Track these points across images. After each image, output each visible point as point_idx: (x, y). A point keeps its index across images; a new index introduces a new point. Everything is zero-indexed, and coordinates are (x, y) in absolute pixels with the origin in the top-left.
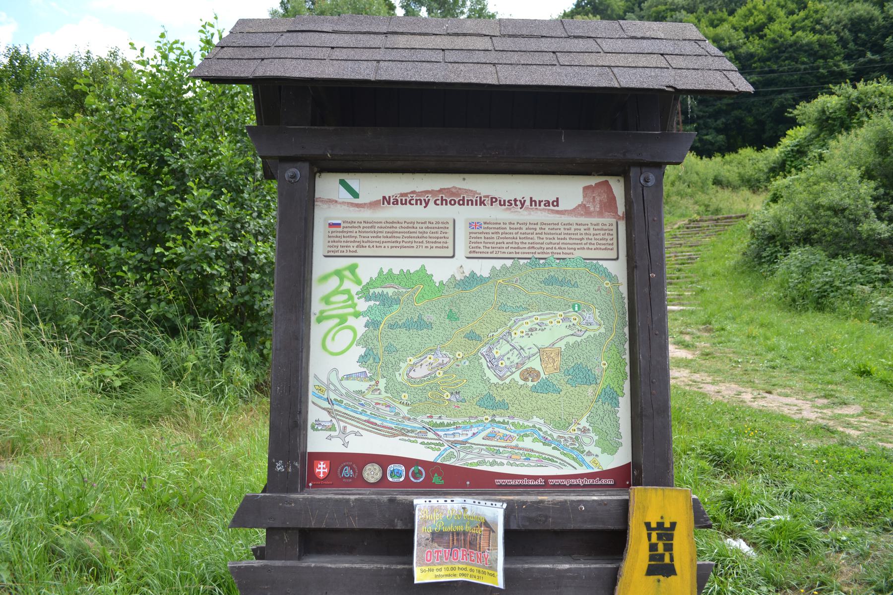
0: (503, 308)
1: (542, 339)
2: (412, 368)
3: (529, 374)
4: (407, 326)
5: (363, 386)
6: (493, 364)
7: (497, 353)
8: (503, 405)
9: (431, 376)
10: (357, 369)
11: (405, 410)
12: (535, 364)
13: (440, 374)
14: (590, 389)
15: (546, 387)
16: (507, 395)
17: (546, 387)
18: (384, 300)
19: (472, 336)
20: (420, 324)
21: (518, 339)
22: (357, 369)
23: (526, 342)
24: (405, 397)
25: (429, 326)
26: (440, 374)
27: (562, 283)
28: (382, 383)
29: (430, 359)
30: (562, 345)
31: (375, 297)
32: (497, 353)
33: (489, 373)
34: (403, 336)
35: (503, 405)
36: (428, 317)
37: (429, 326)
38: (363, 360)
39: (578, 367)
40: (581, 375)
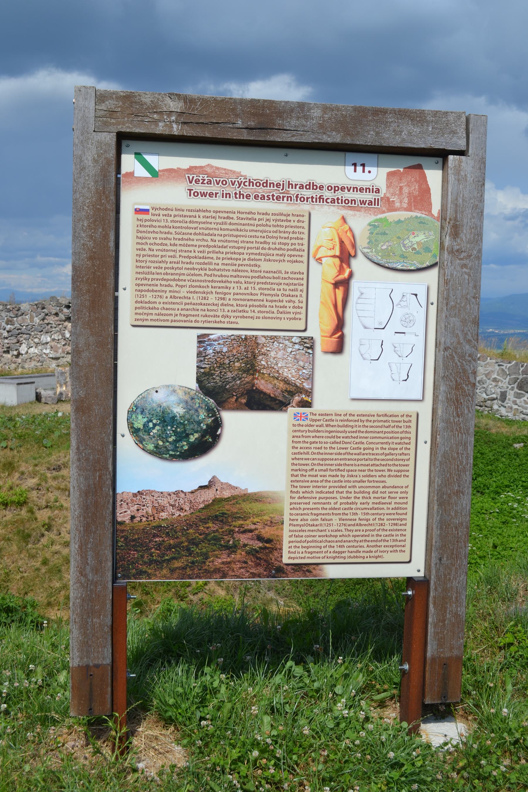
0: (407, 230)
1: (418, 239)
3: (414, 249)
4: (381, 234)
5: (369, 251)
6: (404, 247)
7: (405, 242)
9: (387, 249)
11: (380, 258)
12: (415, 246)
13: (389, 248)
14: (430, 254)
15: (418, 253)
17: (418, 253)
18: (374, 226)
19: (399, 238)
20: (384, 234)
22: (367, 246)
23: (413, 240)
24: (380, 254)
25: (387, 234)
26: (389, 248)
27: (424, 223)
28: (374, 250)
29: (387, 244)
31: (372, 225)
32: (405, 242)
33: (403, 248)
34: (380, 236)
35: (406, 257)
36: (387, 232)
37: (387, 234)
39: (427, 247)
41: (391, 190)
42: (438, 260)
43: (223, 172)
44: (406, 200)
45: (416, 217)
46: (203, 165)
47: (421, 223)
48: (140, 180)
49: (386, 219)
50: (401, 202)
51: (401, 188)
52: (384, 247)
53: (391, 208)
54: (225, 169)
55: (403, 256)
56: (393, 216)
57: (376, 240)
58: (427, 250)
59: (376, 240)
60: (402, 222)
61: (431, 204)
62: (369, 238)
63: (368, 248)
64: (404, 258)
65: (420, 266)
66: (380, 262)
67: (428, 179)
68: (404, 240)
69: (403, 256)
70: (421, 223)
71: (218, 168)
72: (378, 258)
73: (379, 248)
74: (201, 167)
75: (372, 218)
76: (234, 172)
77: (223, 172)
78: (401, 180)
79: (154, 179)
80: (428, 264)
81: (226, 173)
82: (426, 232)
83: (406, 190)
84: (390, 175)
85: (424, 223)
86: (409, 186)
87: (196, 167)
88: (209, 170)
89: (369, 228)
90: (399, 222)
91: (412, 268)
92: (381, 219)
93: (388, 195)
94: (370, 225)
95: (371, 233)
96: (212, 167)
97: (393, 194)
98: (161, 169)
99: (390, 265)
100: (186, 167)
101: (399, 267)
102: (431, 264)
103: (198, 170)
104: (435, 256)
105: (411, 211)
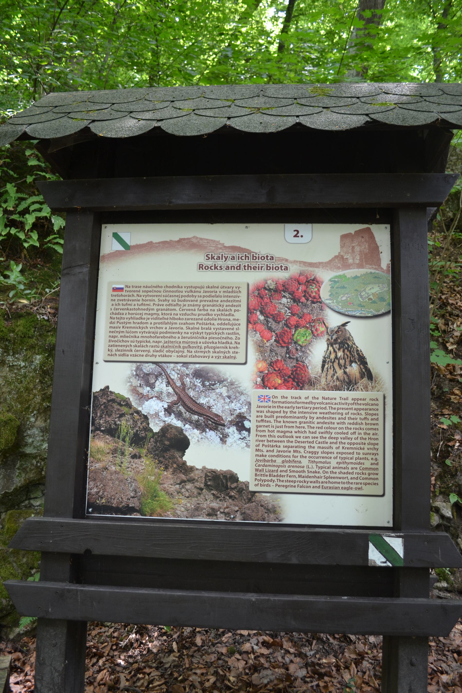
0: (364, 284)
1: (373, 291)
2: (342, 297)
3: (370, 299)
4: (341, 288)
5: (330, 302)
6: (361, 297)
7: (362, 294)
8: (364, 306)
9: (347, 299)
10: (329, 298)
11: (340, 307)
12: (371, 297)
14: (385, 303)
15: (374, 302)
16: (364, 304)
17: (374, 302)
18: (335, 281)
19: (356, 290)
20: (344, 287)
22: (329, 298)
23: (369, 292)
25: (346, 288)
27: (378, 278)
28: (335, 301)
29: (346, 295)
30: (378, 292)
31: (333, 281)
32: (362, 294)
33: (360, 299)
34: (340, 290)
35: (364, 306)
36: (346, 286)
37: (346, 288)
38: (330, 295)
39: (382, 298)
41: (345, 249)
43: (206, 241)
44: (358, 257)
45: (371, 273)
47: (375, 277)
49: (344, 276)
50: (353, 259)
51: (353, 247)
53: (346, 266)
54: (207, 240)
57: (336, 293)
58: (382, 299)
59: (336, 293)
60: (359, 277)
61: (379, 260)
62: (330, 291)
63: (330, 299)
64: (362, 307)
65: (376, 313)
66: (341, 311)
69: (361, 305)
71: (201, 239)
72: (339, 308)
73: (339, 300)
74: (188, 239)
76: (214, 241)
80: (383, 311)
81: (208, 243)
82: (380, 285)
83: (357, 249)
84: (344, 237)
85: (378, 278)
86: (360, 245)
88: (194, 241)
89: (330, 283)
90: (356, 277)
91: (370, 315)
92: (340, 276)
93: (342, 254)
94: (330, 280)
95: (332, 287)
96: (197, 238)
97: (347, 253)
99: (350, 313)
100: (177, 239)
101: (358, 314)
103: (186, 241)
105: (363, 268)
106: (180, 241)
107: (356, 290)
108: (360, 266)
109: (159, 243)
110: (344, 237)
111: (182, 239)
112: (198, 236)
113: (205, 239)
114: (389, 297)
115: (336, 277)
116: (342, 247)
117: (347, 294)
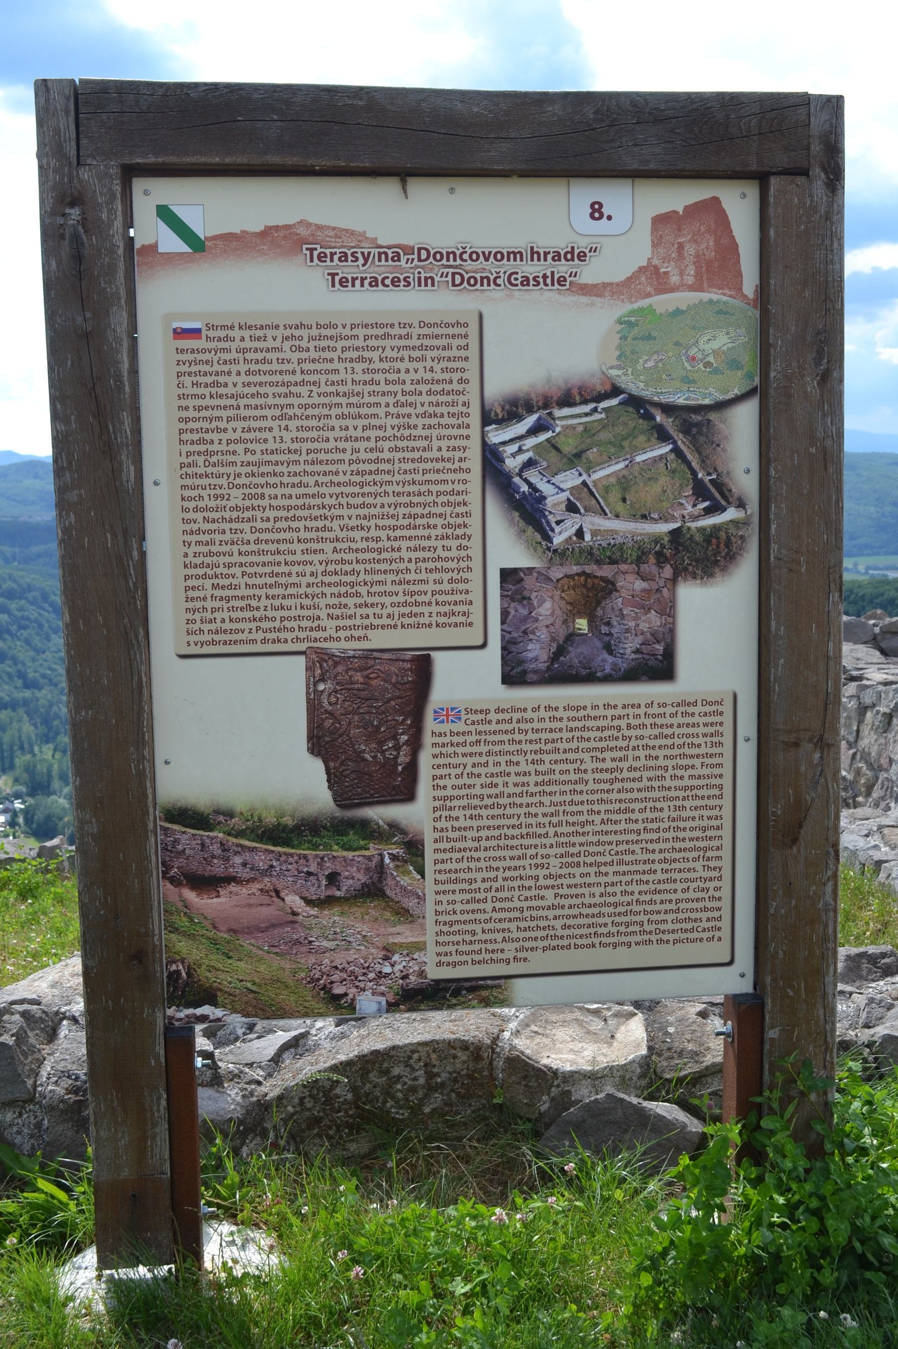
0: (693, 328)
1: (715, 345)
3: (708, 364)
4: (642, 339)
5: (620, 372)
8: (694, 382)
9: (656, 366)
11: (642, 385)
12: (711, 359)
17: (716, 371)
18: (630, 324)
19: (677, 344)
20: (649, 337)
21: (702, 345)
22: (616, 363)
29: (655, 357)
35: (694, 382)
36: (654, 334)
38: (619, 358)
40: (735, 365)
41: (661, 251)
42: (757, 381)
43: (331, 233)
46: (291, 222)
47: (720, 312)
48: (171, 258)
51: (681, 246)
52: (650, 364)
53: (662, 285)
55: (687, 380)
56: (664, 302)
57: (633, 352)
59: (633, 352)
62: (619, 347)
63: (619, 367)
64: (690, 382)
65: (721, 398)
67: (733, 226)
68: (688, 349)
69: (687, 380)
70: (720, 312)
71: (320, 227)
73: (639, 367)
74: (287, 227)
75: (624, 308)
76: (352, 233)
77: (331, 233)
78: (679, 230)
79: (197, 255)
80: (736, 391)
81: (337, 237)
83: (690, 250)
86: (696, 241)
87: (277, 228)
88: (303, 232)
90: (678, 312)
91: (707, 402)
92: (641, 309)
94: (620, 321)
95: (624, 338)
96: (309, 225)
98: (210, 234)
100: (258, 228)
102: (744, 391)
104: (750, 376)
105: (702, 291)
106: (268, 232)
107: (677, 344)
108: (697, 287)
109: (214, 238)
110: (660, 221)
111: (271, 228)
112: (311, 220)
113: (329, 227)
114: (749, 360)
115: (632, 313)
116: (655, 246)
117: (657, 352)
